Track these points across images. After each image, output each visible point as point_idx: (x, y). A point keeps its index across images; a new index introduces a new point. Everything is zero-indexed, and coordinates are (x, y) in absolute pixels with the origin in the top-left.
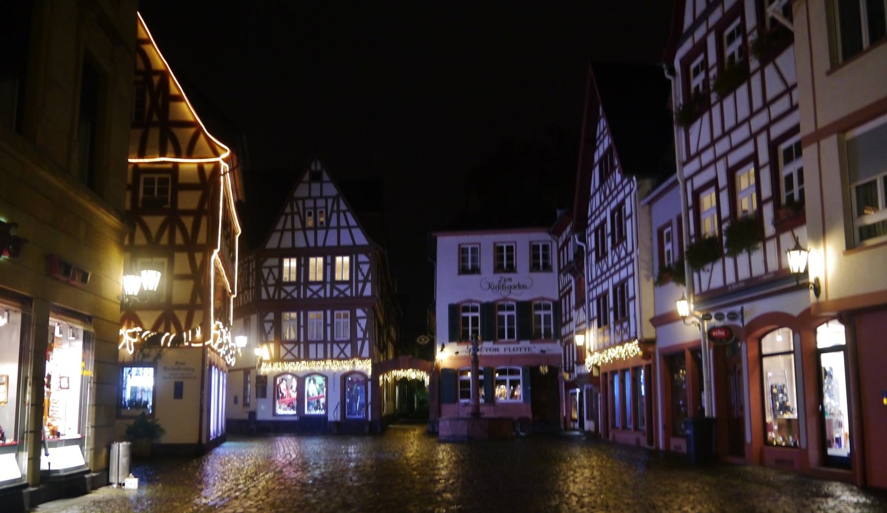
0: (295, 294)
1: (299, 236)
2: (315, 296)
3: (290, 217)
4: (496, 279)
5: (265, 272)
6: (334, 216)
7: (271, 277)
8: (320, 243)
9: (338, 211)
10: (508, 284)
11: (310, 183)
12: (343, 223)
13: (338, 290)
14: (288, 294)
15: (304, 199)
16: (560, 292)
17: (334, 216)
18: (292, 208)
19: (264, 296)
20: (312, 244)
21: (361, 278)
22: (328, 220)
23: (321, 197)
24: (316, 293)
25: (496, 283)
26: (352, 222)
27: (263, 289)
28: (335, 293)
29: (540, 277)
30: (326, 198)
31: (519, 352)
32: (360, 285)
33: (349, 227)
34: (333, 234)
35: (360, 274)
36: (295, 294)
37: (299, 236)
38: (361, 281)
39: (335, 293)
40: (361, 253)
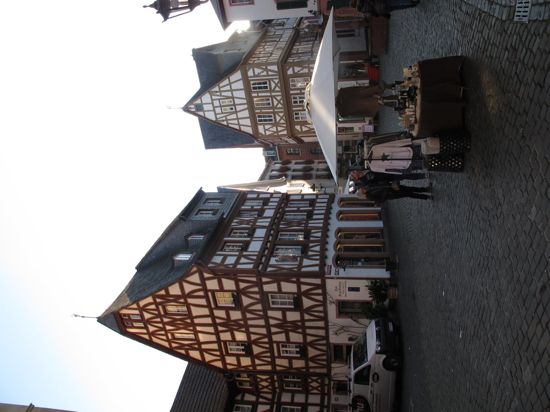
0: (281, 114)
1: (240, 115)
2: (282, 102)
3: (229, 122)
5: (268, 133)
6: (223, 94)
7: (271, 129)
8: (245, 101)
9: (220, 92)
11: (204, 111)
12: (228, 88)
13: (275, 88)
14: (282, 118)
15: (216, 114)
17: (223, 94)
18: (223, 121)
19: (285, 132)
20: (246, 106)
21: (265, 73)
22: (228, 98)
23: (212, 103)
24: (279, 102)
26: (226, 82)
27: (279, 134)
28: (277, 89)
30: (212, 100)
32: (270, 73)
33: (230, 84)
34: (236, 94)
35: (262, 74)
36: (281, 114)
37: (240, 115)
38: (267, 73)
39: (277, 89)
40: (247, 74)
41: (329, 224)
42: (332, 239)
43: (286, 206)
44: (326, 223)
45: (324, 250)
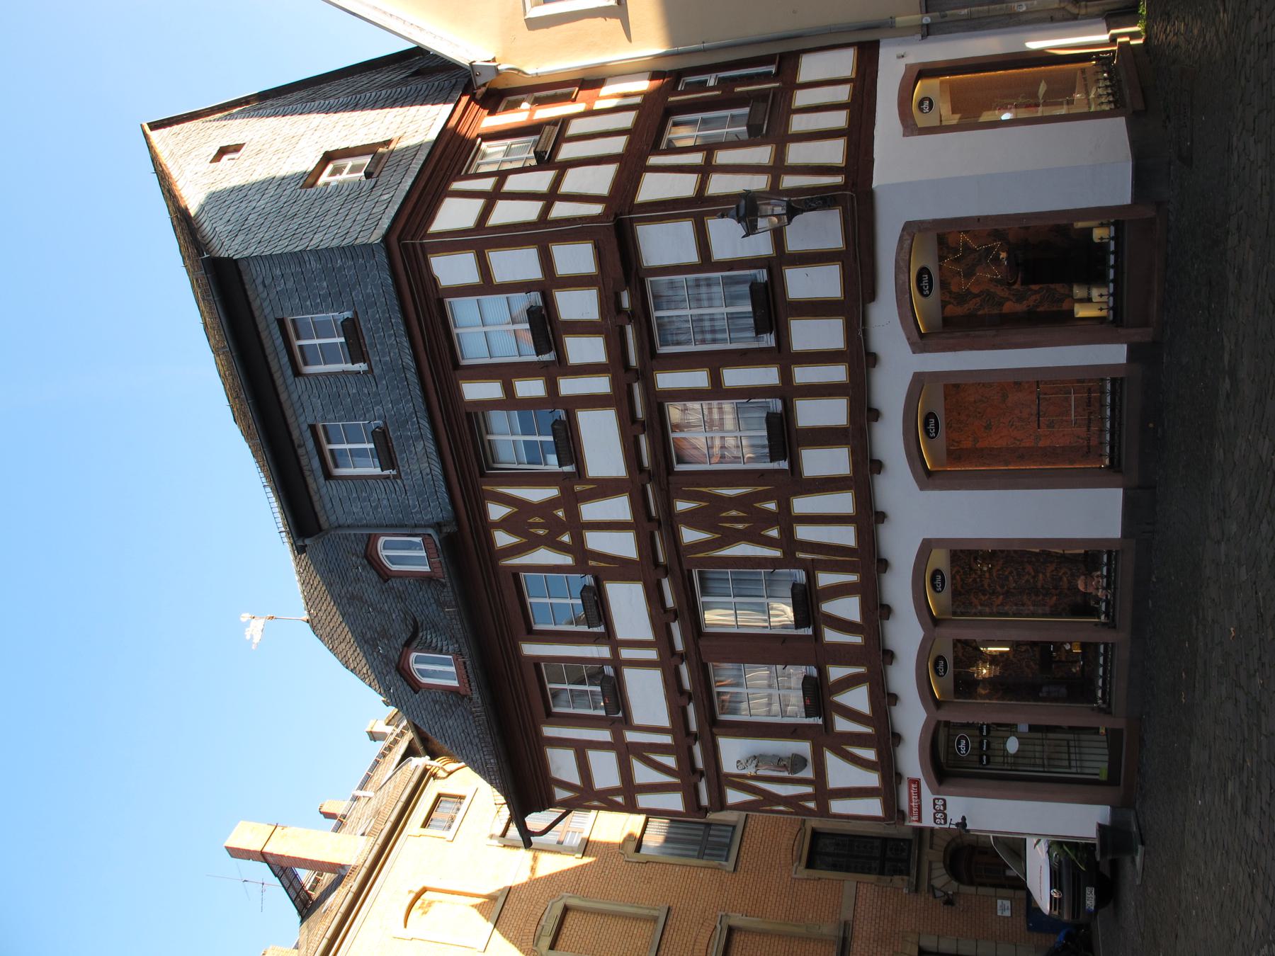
41: (881, 517)
42: (906, 634)
43: (653, 360)
44: (869, 517)
45: (884, 699)
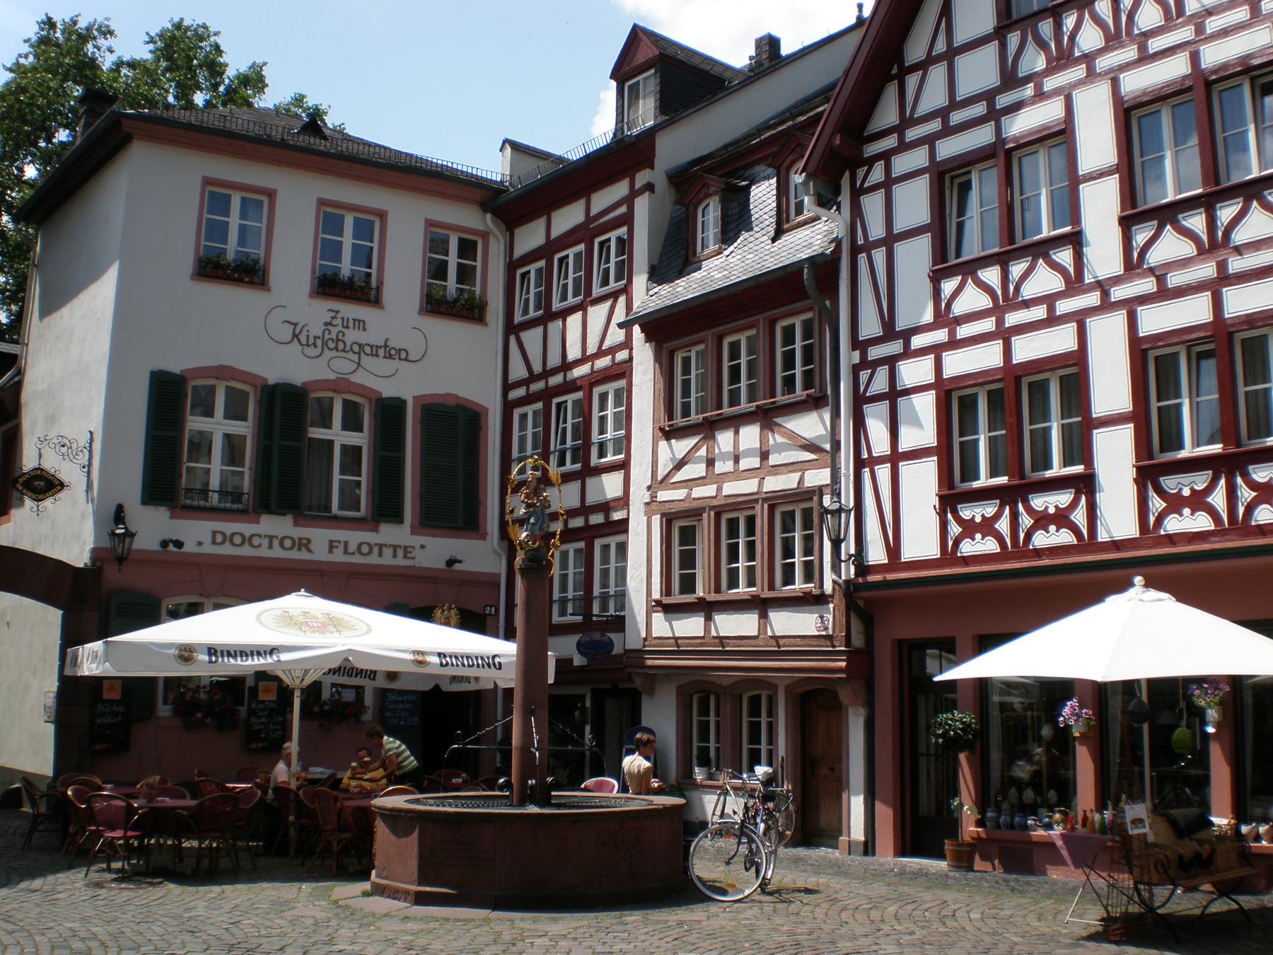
4: (317, 313)
10: (352, 336)
16: (507, 387)
25: (317, 329)
29: (450, 334)
31: (374, 559)
